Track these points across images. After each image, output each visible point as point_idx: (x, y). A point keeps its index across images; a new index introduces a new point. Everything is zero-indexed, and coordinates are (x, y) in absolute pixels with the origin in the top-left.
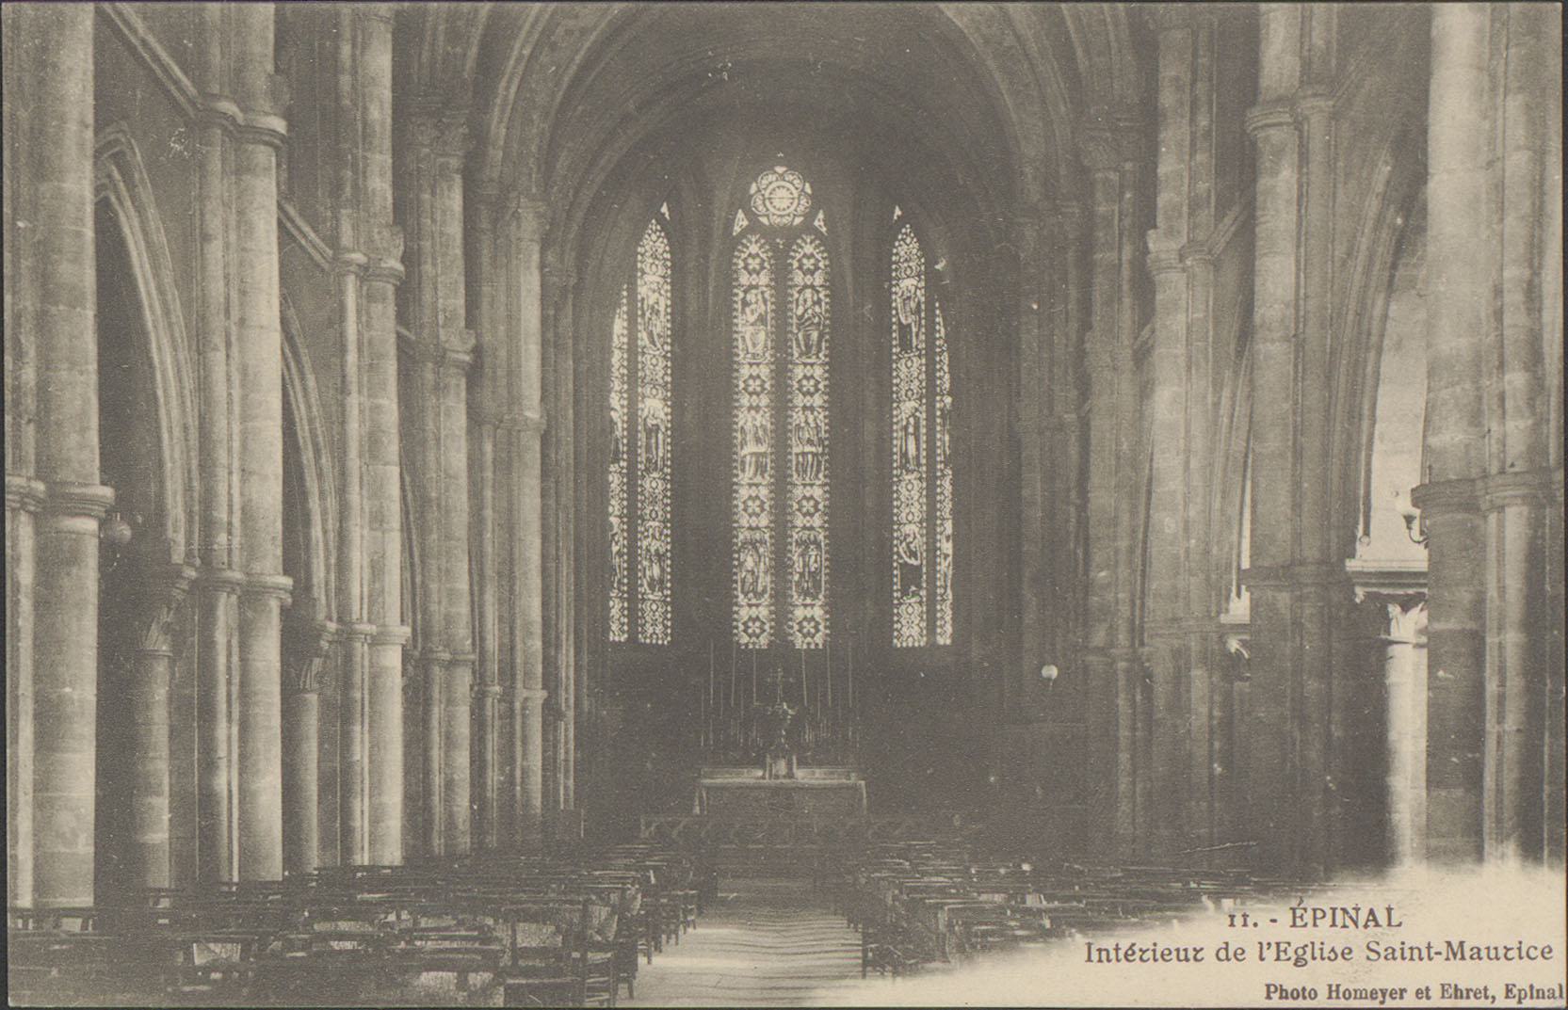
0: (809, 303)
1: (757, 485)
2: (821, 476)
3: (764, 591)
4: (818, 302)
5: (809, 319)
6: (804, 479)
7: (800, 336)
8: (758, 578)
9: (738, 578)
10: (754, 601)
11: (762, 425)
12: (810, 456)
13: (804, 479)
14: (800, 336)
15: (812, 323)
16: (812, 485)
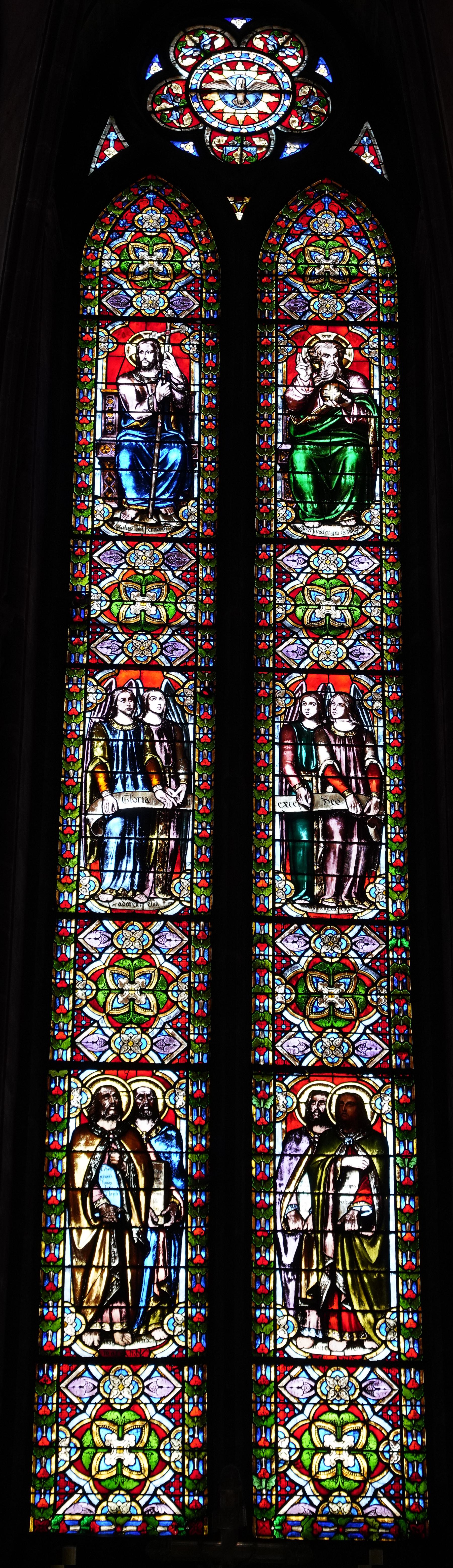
0: (330, 369)
1: (146, 918)
2: (376, 889)
3: (168, 1301)
4: (361, 368)
5: (329, 412)
6: (315, 902)
7: (300, 458)
8: (141, 1249)
9: (63, 1251)
10: (120, 1343)
11: (167, 728)
12: (335, 825)
13: (315, 902)
14: (300, 458)
15: (341, 423)
16: (342, 923)
